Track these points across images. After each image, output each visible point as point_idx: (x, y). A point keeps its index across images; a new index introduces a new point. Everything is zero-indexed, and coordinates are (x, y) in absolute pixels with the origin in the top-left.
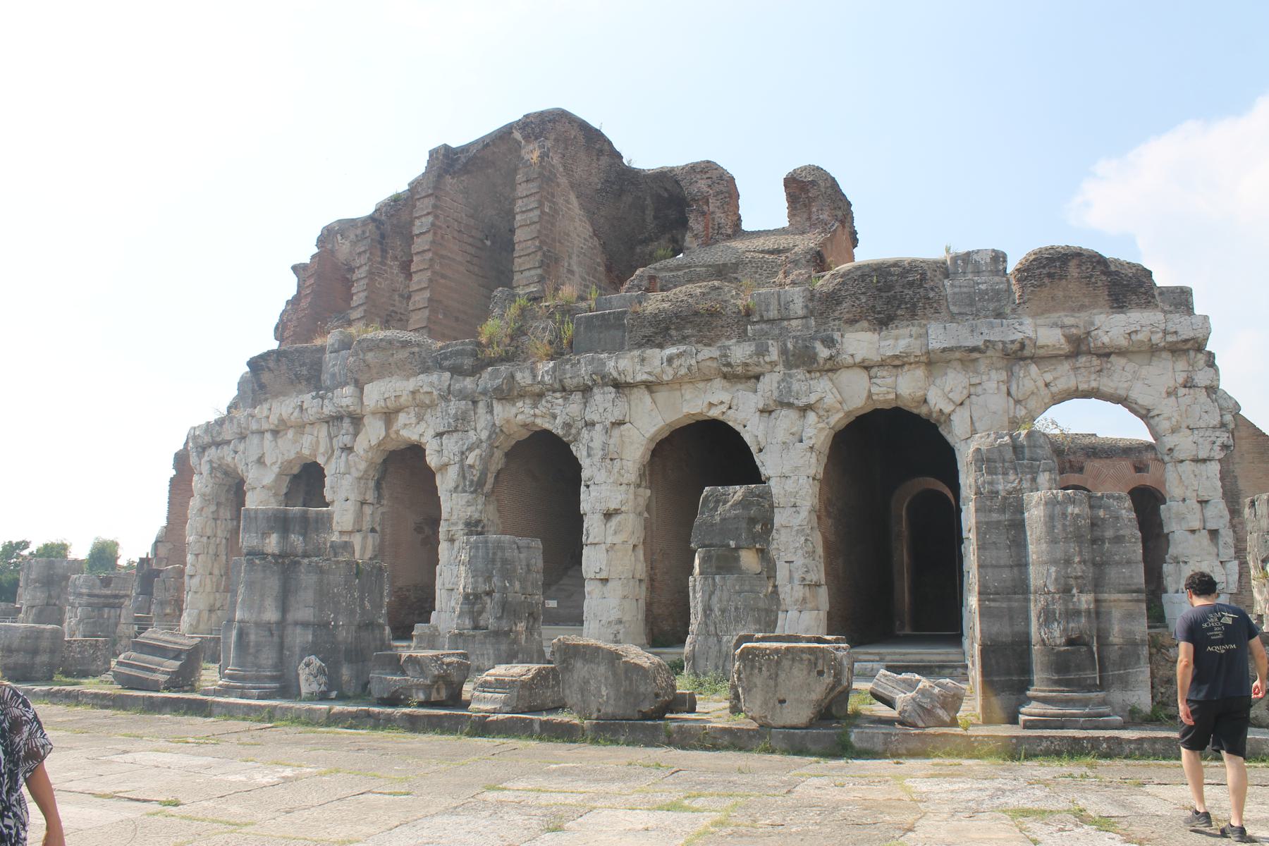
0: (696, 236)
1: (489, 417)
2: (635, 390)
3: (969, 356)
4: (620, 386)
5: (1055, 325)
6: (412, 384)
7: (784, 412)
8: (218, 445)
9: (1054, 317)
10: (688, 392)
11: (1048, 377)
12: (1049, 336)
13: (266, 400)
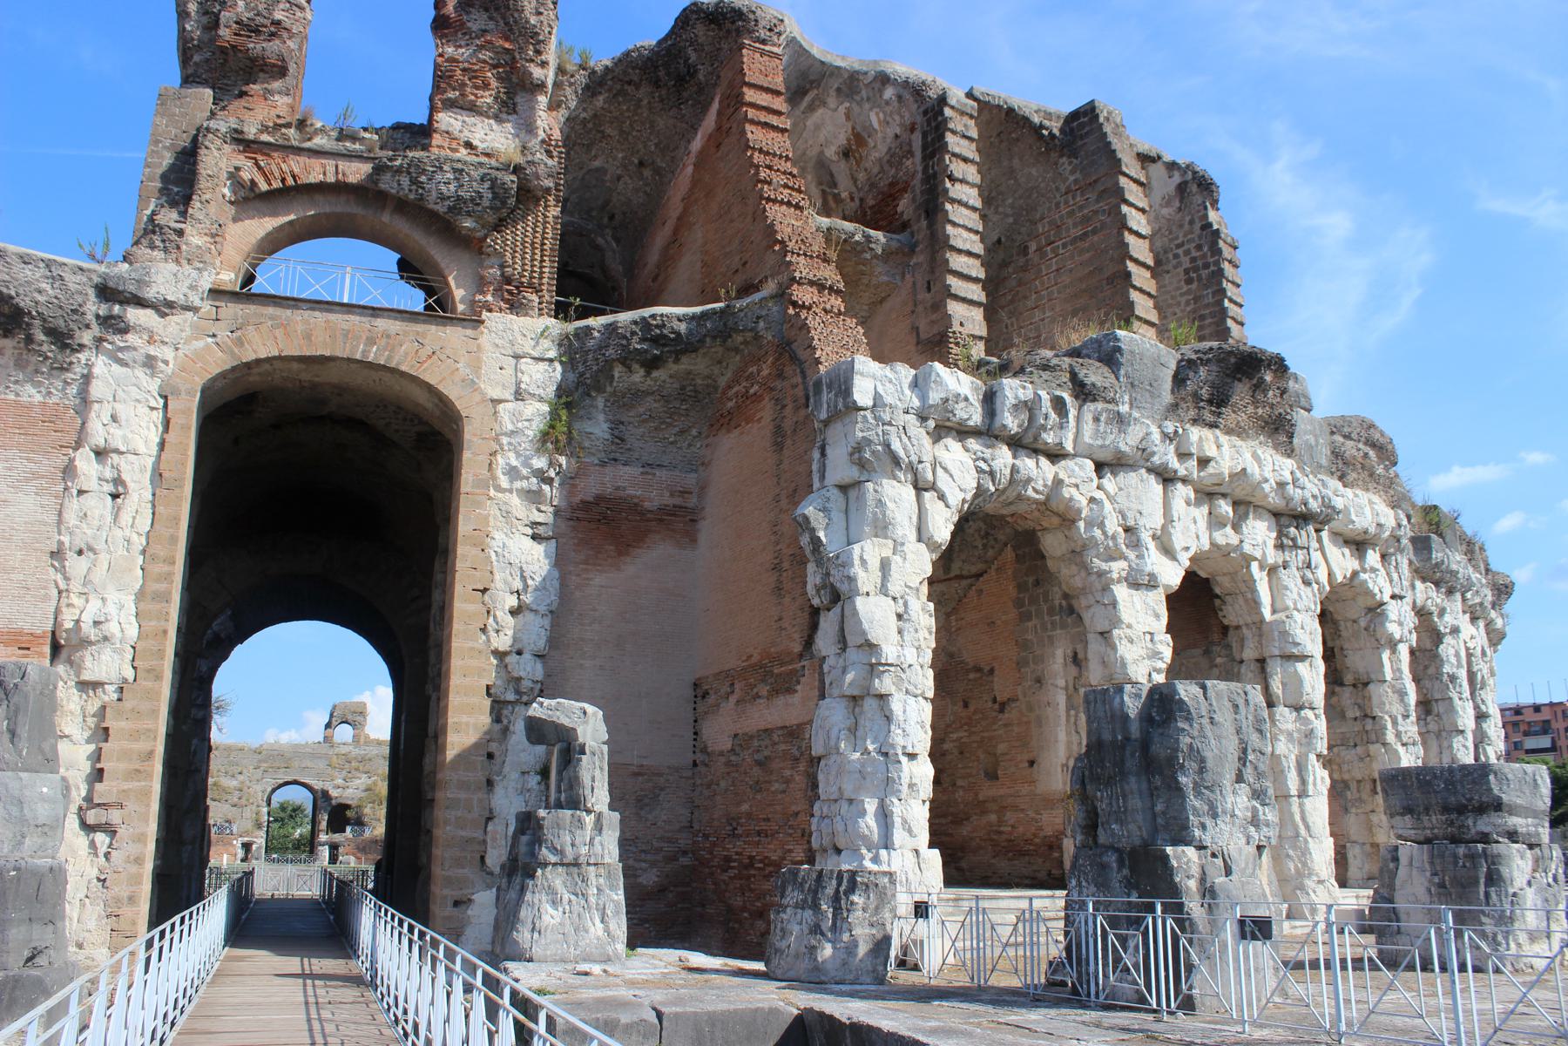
13: (1213, 426)
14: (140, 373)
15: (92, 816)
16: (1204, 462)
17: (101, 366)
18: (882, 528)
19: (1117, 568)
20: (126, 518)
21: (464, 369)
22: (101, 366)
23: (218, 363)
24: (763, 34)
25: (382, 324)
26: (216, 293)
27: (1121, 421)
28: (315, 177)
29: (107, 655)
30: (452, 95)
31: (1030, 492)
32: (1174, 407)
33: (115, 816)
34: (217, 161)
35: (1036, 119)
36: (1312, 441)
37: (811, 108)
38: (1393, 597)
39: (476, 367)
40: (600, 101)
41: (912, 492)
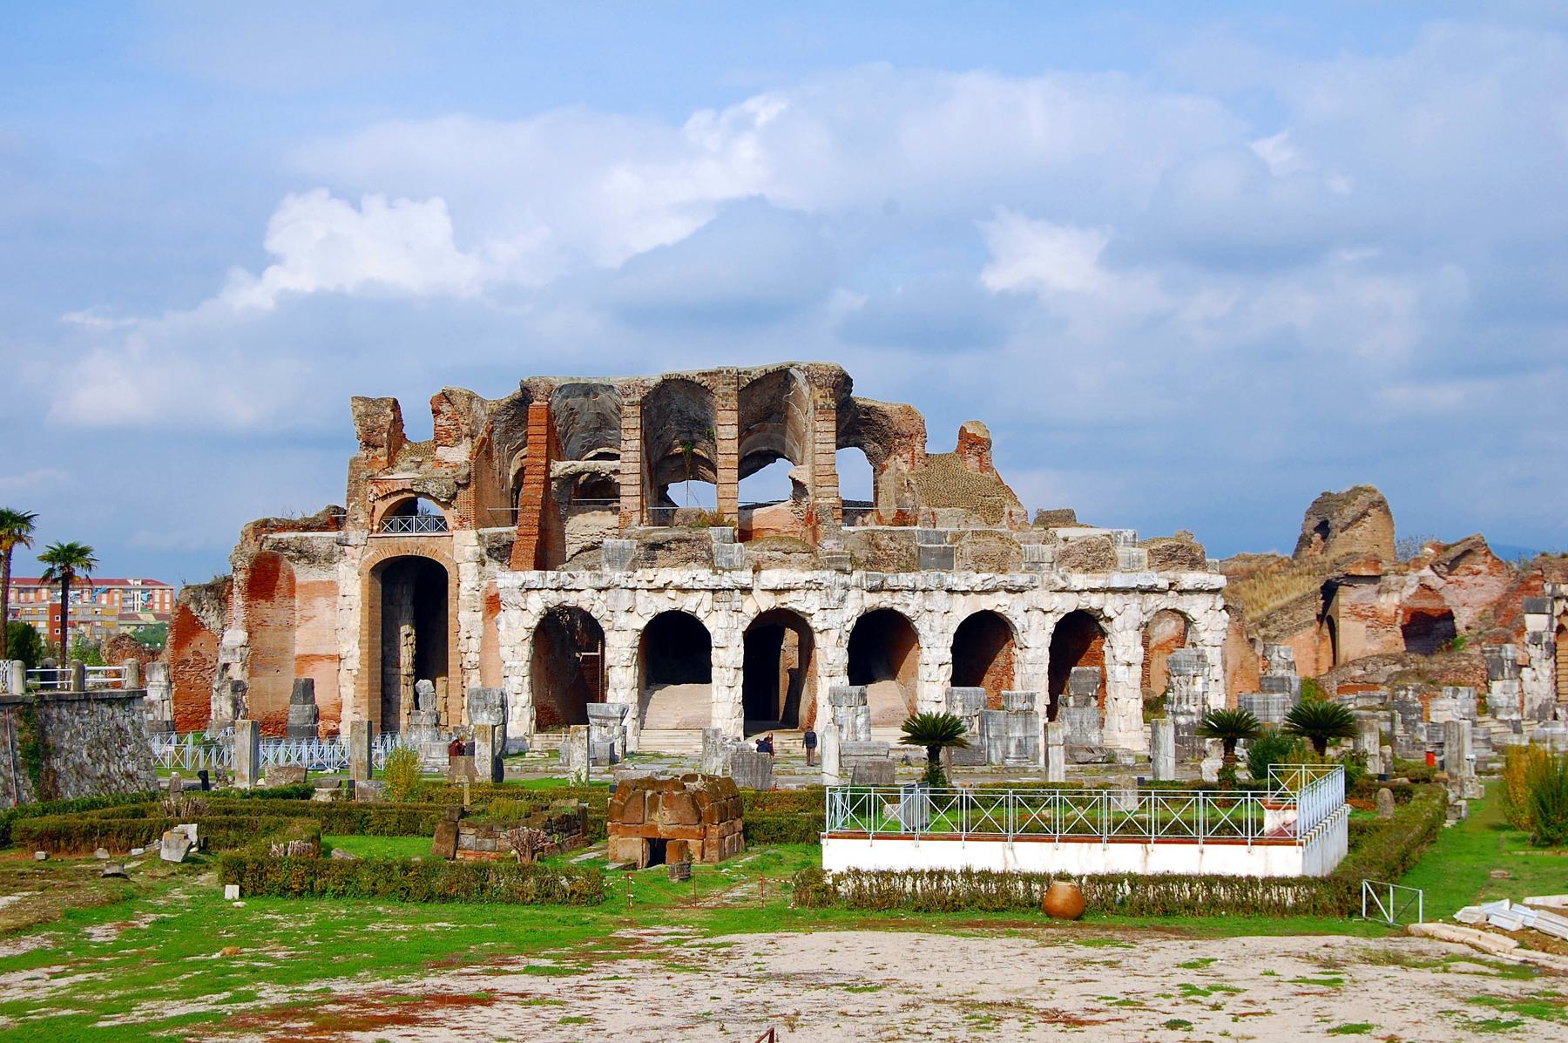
0: (906, 462)
1: (859, 601)
2: (955, 595)
6: (808, 576)
7: (1036, 612)
10: (983, 597)
11: (1158, 602)
12: (1163, 584)
27: (600, 577)
30: (439, 442)
31: (567, 605)
39: (452, 552)
41: (520, 611)
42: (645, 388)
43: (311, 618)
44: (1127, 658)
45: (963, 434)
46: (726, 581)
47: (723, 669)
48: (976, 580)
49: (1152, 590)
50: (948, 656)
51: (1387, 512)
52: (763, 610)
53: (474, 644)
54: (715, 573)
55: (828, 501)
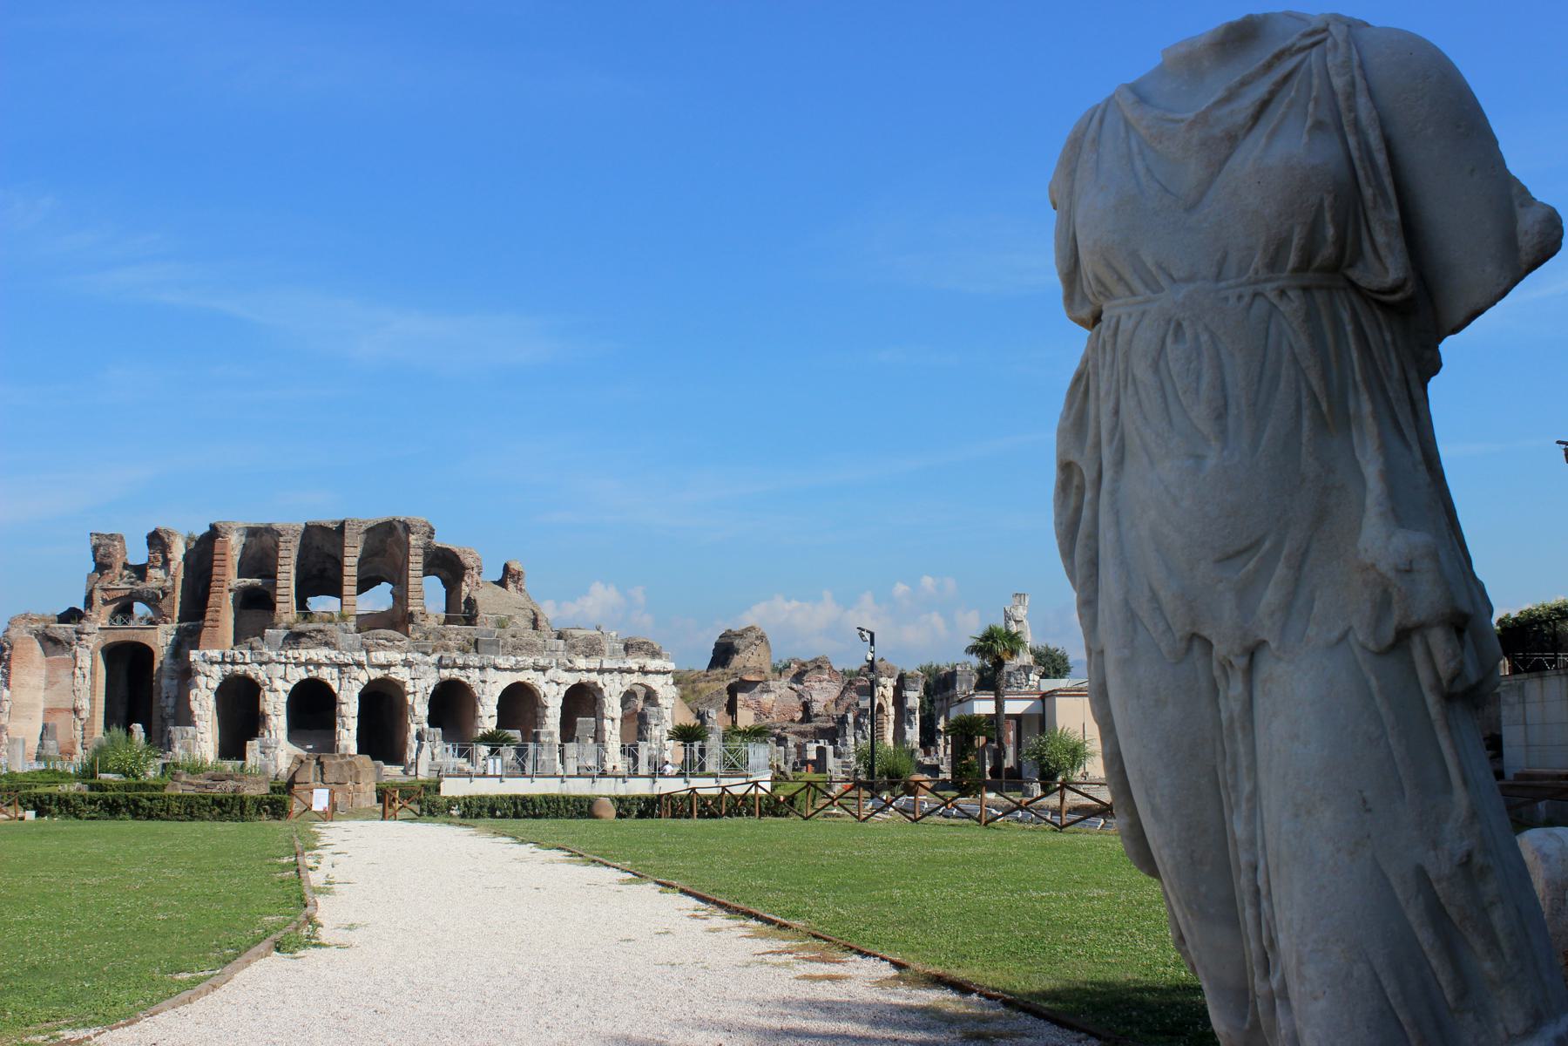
0: (468, 586)
3: (611, 671)
4: (496, 668)
5: (637, 663)
8: (233, 663)
9: (637, 660)
12: (635, 667)
14: (86, 649)
15: (84, 746)
16: (295, 658)
17: (78, 649)
18: (197, 687)
19: (265, 688)
20: (86, 682)
21: (154, 639)
22: (78, 649)
23: (102, 645)
24: (223, 535)
25: (135, 631)
26: (100, 628)
28: (120, 595)
29: (84, 713)
32: (282, 647)
33: (88, 746)
34: (98, 595)
35: (331, 526)
36: (351, 642)
37: (262, 535)
38: (413, 679)
39: (157, 640)
40: (202, 545)
41: (206, 678)
42: (295, 531)
43: (56, 683)
44: (612, 715)
45: (506, 568)
46: (348, 658)
47: (345, 719)
48: (512, 660)
49: (630, 671)
50: (495, 712)
51: (767, 643)
52: (372, 678)
53: (171, 702)
54: (340, 653)
55: (416, 608)
